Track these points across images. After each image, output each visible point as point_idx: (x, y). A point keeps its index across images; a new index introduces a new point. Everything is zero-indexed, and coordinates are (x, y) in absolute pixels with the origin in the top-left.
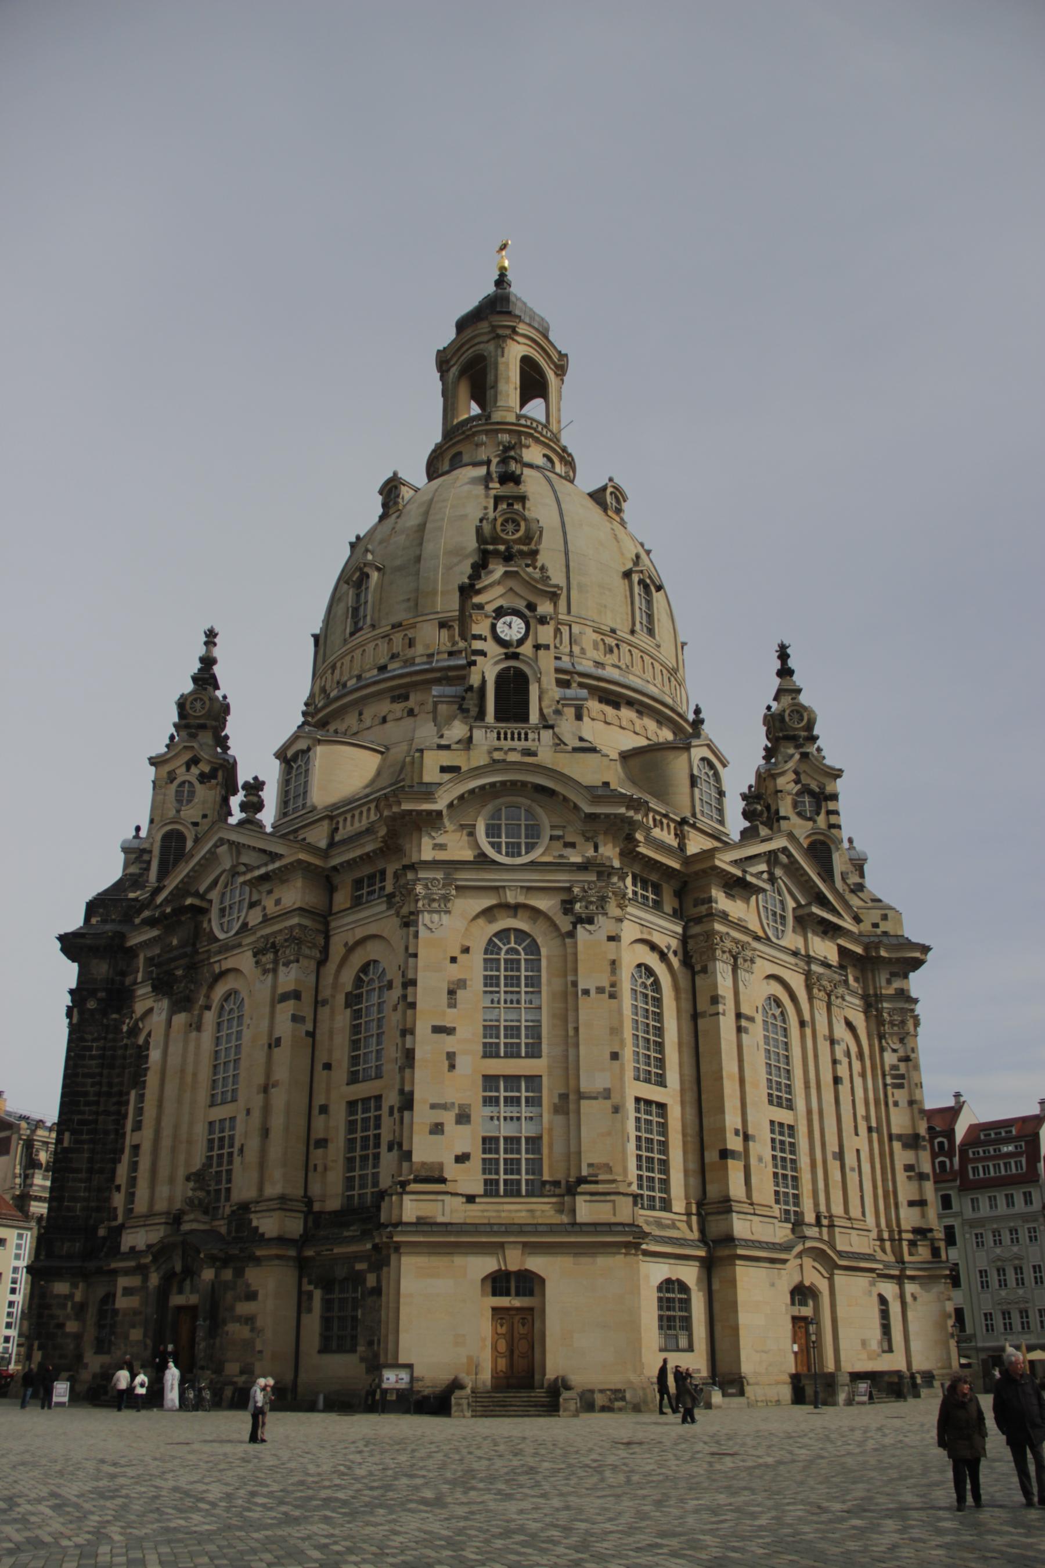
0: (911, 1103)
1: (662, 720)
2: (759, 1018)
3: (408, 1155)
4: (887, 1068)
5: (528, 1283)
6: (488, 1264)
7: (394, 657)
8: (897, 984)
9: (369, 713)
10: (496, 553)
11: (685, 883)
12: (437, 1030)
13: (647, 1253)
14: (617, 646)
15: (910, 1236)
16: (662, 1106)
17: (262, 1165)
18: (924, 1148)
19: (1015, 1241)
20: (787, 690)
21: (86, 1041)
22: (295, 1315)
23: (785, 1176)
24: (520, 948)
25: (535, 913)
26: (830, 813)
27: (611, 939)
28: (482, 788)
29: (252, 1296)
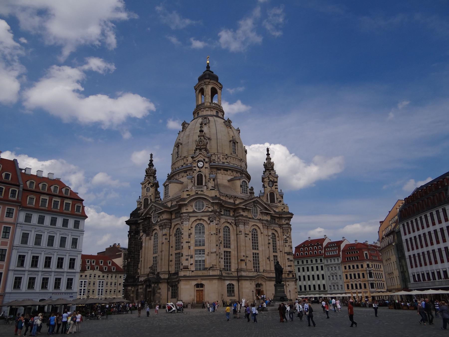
0: (289, 246)
1: (237, 172)
3: (182, 264)
5: (202, 285)
6: (195, 283)
7: (184, 163)
8: (287, 222)
9: (180, 175)
10: (198, 148)
12: (187, 242)
13: (224, 280)
17: (161, 265)
19: (335, 269)
20: (268, 159)
23: (256, 263)
29: (160, 289)
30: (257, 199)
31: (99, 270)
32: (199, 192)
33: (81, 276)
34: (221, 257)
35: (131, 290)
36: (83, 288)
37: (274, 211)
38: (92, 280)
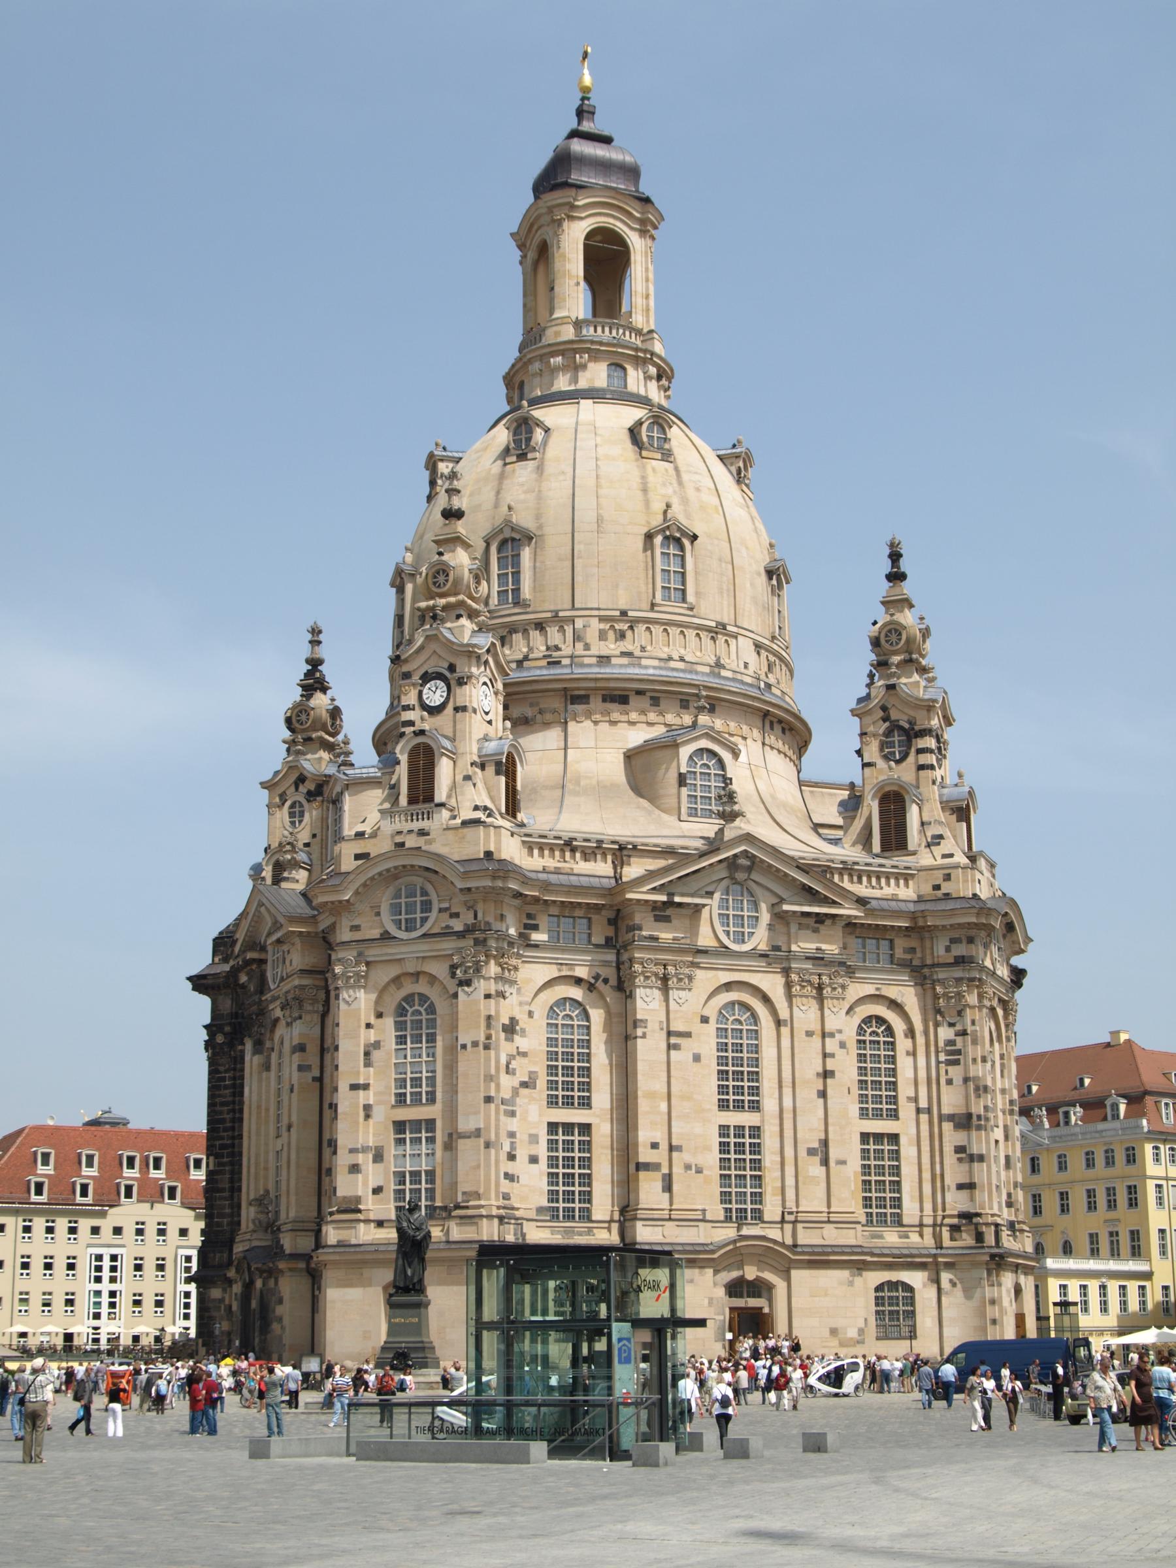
0: (966, 1080)
2: (712, 1026)
4: (941, 1044)
11: (618, 911)
12: (354, 1087)
14: (631, 628)
15: (955, 1221)
16: (586, 1128)
18: (979, 1128)
21: (220, 1072)
22: (310, 1315)
24: (422, 1010)
25: (433, 979)
26: (920, 751)
27: (488, 996)
28: (380, 874)
30: (743, 848)
31: (184, 1205)
32: (411, 842)
33: (95, 1230)
34: (522, 1154)
35: (222, 1300)
36: (105, 1287)
37: (861, 901)
38: (151, 1249)
